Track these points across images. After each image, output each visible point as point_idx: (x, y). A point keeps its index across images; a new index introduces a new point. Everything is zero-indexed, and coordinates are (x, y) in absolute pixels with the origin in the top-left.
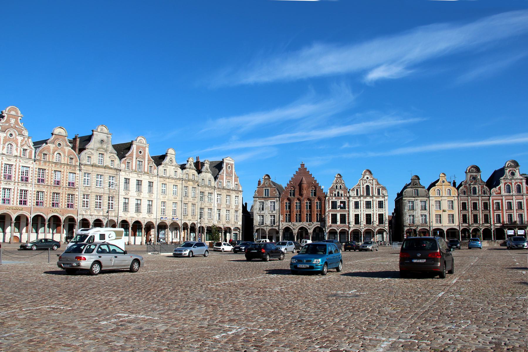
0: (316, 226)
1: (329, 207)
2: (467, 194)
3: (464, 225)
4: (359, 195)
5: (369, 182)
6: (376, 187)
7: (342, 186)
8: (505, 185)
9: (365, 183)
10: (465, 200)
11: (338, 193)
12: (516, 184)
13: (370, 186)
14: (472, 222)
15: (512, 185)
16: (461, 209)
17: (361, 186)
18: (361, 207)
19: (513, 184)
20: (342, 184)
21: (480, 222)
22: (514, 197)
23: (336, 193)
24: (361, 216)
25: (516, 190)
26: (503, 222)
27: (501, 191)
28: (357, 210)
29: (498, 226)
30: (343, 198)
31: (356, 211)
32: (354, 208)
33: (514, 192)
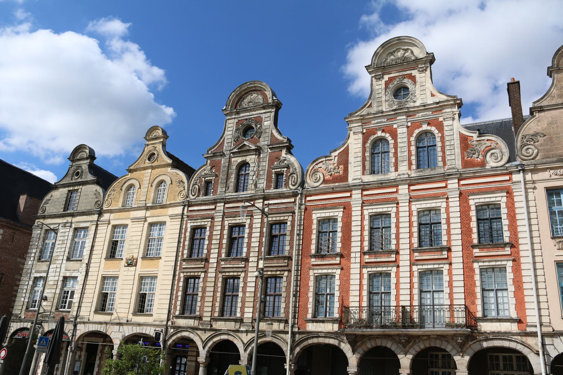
2: (215, 193)
3: (182, 322)
8: (364, 143)
10: (204, 218)
12: (417, 131)
14: (212, 311)
15: (394, 135)
16: (183, 254)
19: (402, 131)
21: (243, 313)
22: (403, 189)
25: (413, 158)
26: (345, 309)
27: (346, 170)
29: (316, 335)
33: (403, 168)
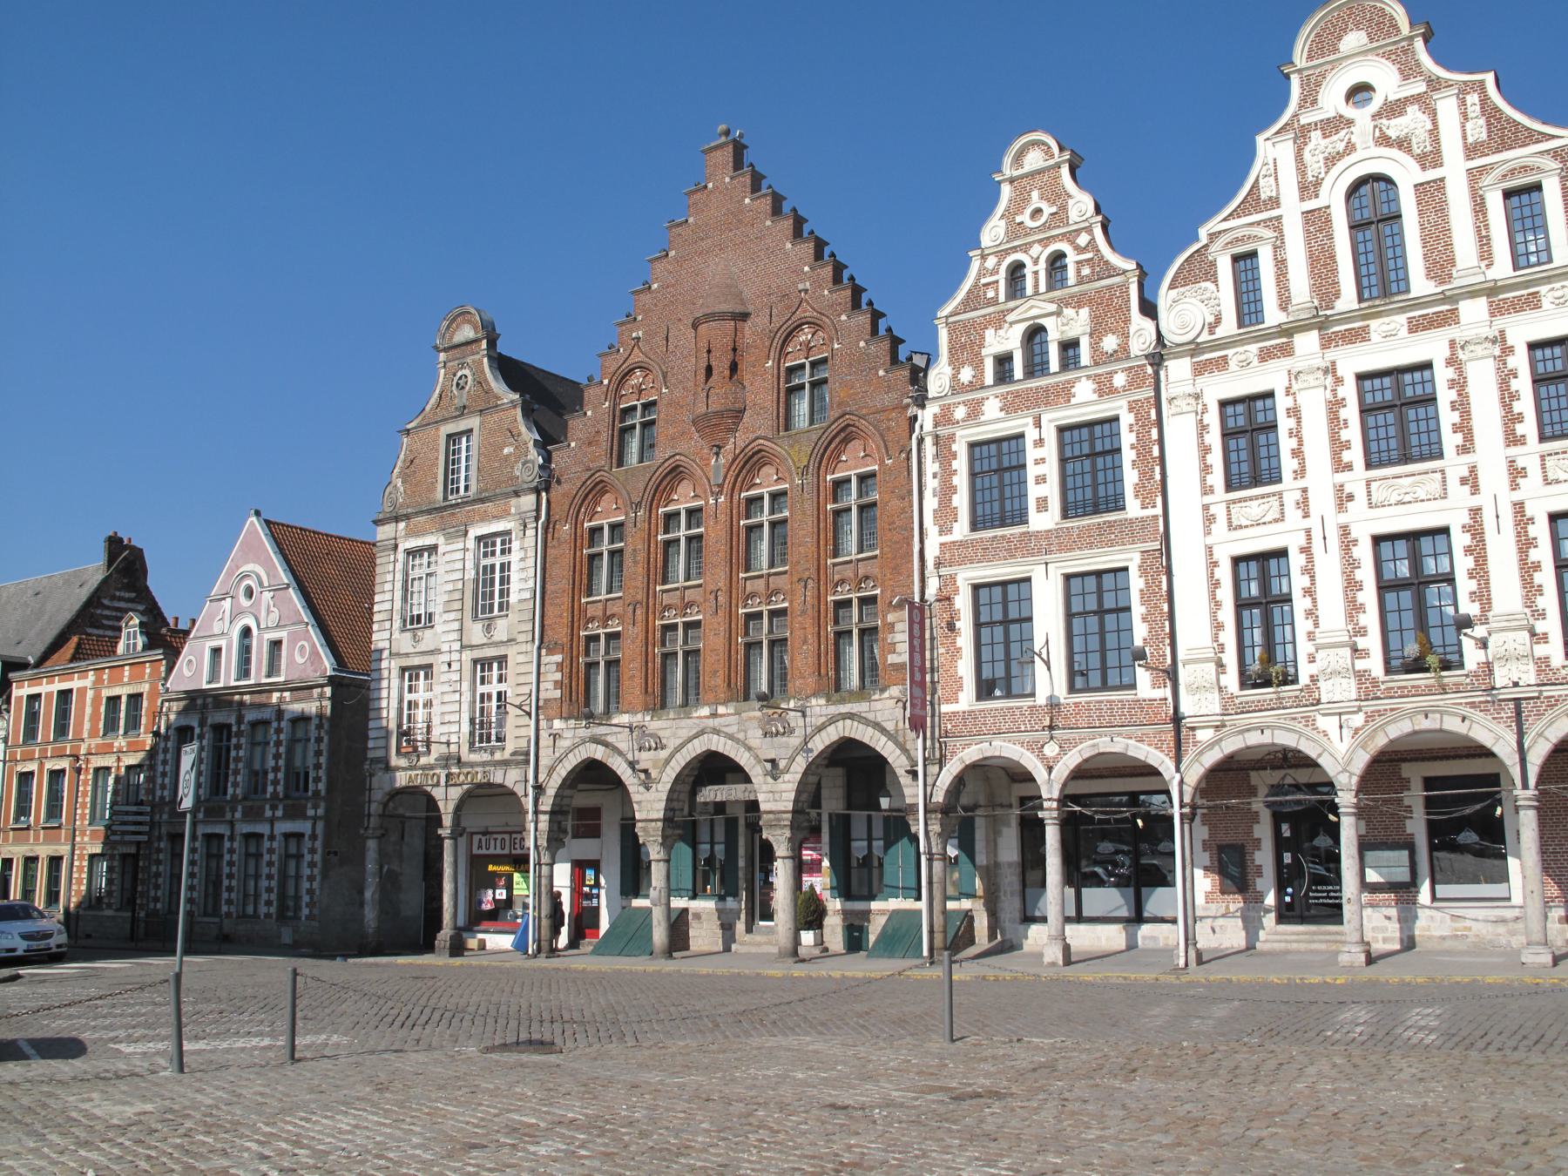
0: (832, 735)
1: (946, 515)
4: (1273, 316)
5: (1384, 140)
6: (1474, 175)
7: (1071, 258)
9: (1331, 161)
11: (1035, 333)
13: (1406, 174)
17: (1292, 210)
18: (1297, 453)
20: (1070, 237)
23: (1010, 339)
24: (1309, 571)
28: (1254, 504)
30: (1084, 390)
31: (1255, 510)
32: (1217, 478)
